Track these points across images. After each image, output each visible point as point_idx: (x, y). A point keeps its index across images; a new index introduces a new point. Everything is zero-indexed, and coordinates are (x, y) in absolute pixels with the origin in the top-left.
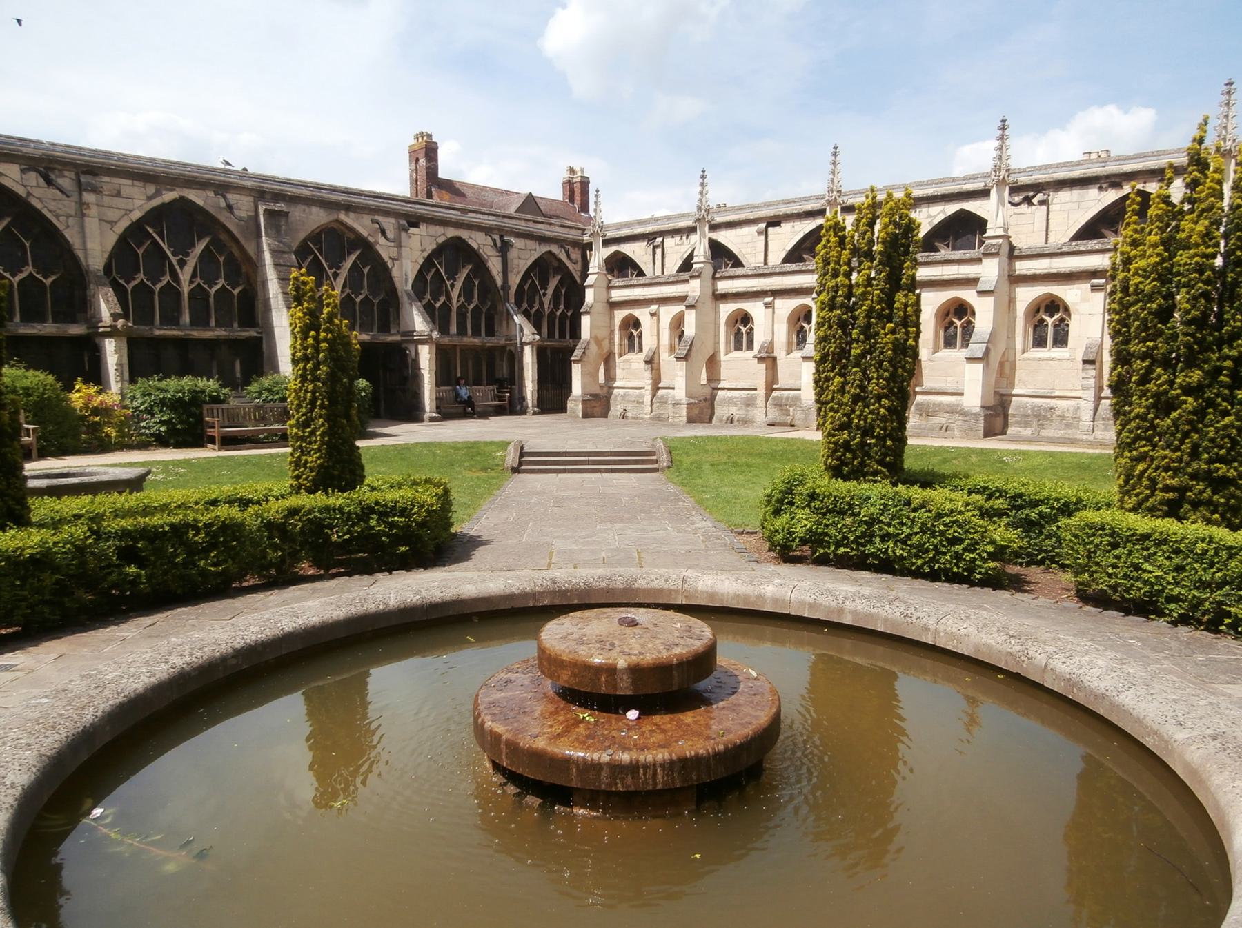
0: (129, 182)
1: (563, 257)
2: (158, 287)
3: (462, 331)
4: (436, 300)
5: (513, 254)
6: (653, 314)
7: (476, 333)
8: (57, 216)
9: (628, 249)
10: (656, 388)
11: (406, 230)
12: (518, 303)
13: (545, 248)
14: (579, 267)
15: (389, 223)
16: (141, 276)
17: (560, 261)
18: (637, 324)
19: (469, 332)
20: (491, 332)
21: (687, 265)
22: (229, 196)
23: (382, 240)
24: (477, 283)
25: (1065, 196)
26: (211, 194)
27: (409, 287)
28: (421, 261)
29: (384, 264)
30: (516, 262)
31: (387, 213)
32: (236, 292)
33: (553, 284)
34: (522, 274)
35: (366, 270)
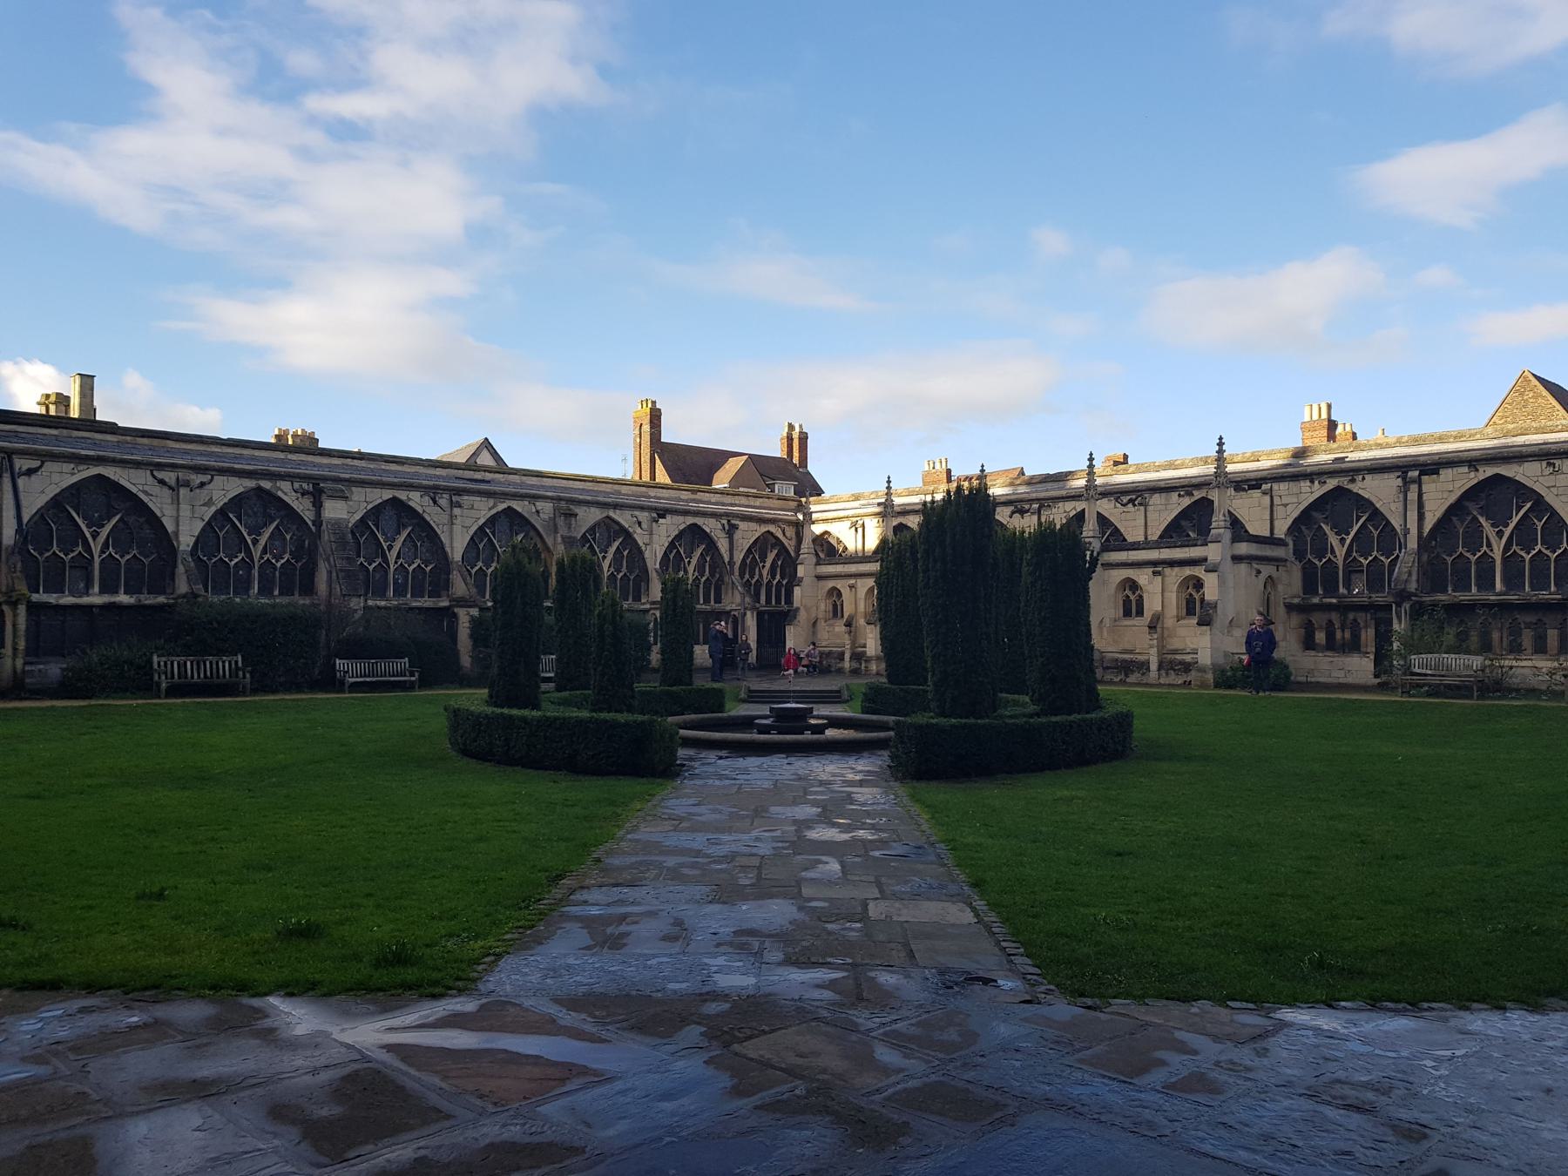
0: (479, 499)
1: (779, 535)
2: (490, 570)
5: (737, 535)
6: (851, 587)
8: (438, 525)
13: (764, 528)
14: (793, 543)
15: (644, 516)
16: (480, 564)
18: (839, 594)
20: (718, 600)
22: (537, 504)
23: (639, 530)
24: (708, 559)
25: (1156, 499)
26: (527, 503)
27: (658, 566)
28: (666, 544)
29: (639, 548)
31: (642, 508)
34: (745, 551)
35: (625, 553)
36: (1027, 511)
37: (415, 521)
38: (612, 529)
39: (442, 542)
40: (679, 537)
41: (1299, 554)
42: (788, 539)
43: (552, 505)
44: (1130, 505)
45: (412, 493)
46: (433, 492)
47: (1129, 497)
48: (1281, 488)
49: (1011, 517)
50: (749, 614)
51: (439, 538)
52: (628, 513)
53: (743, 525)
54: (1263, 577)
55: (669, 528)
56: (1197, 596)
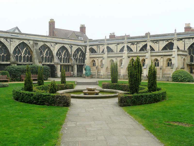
1: (81, 48)
3: (64, 62)
4: (59, 57)
5: (73, 48)
6: (97, 60)
7: (66, 62)
9: (93, 47)
10: (98, 72)
11: (55, 45)
12: (73, 57)
13: (78, 47)
14: (84, 50)
15: (53, 44)
16: (17, 54)
17: (81, 49)
18: (95, 61)
19: (65, 62)
20: (68, 62)
21: (103, 52)
23: (51, 47)
25: (161, 42)
29: (51, 51)
30: (73, 50)
32: (29, 56)
33: (80, 53)
36: (134, 44)
37: (2, 45)
38: (45, 47)
39: (8, 49)
40: (60, 49)
41: (190, 54)
42: (83, 49)
43: (32, 41)
44: (156, 43)
45: (1, 38)
46: (6, 38)
47: (155, 42)
48: (187, 40)
49: (131, 45)
50: (75, 65)
51: (8, 49)
52: (49, 43)
53: (74, 46)
54: (183, 58)
55: (58, 47)
56: (170, 62)
